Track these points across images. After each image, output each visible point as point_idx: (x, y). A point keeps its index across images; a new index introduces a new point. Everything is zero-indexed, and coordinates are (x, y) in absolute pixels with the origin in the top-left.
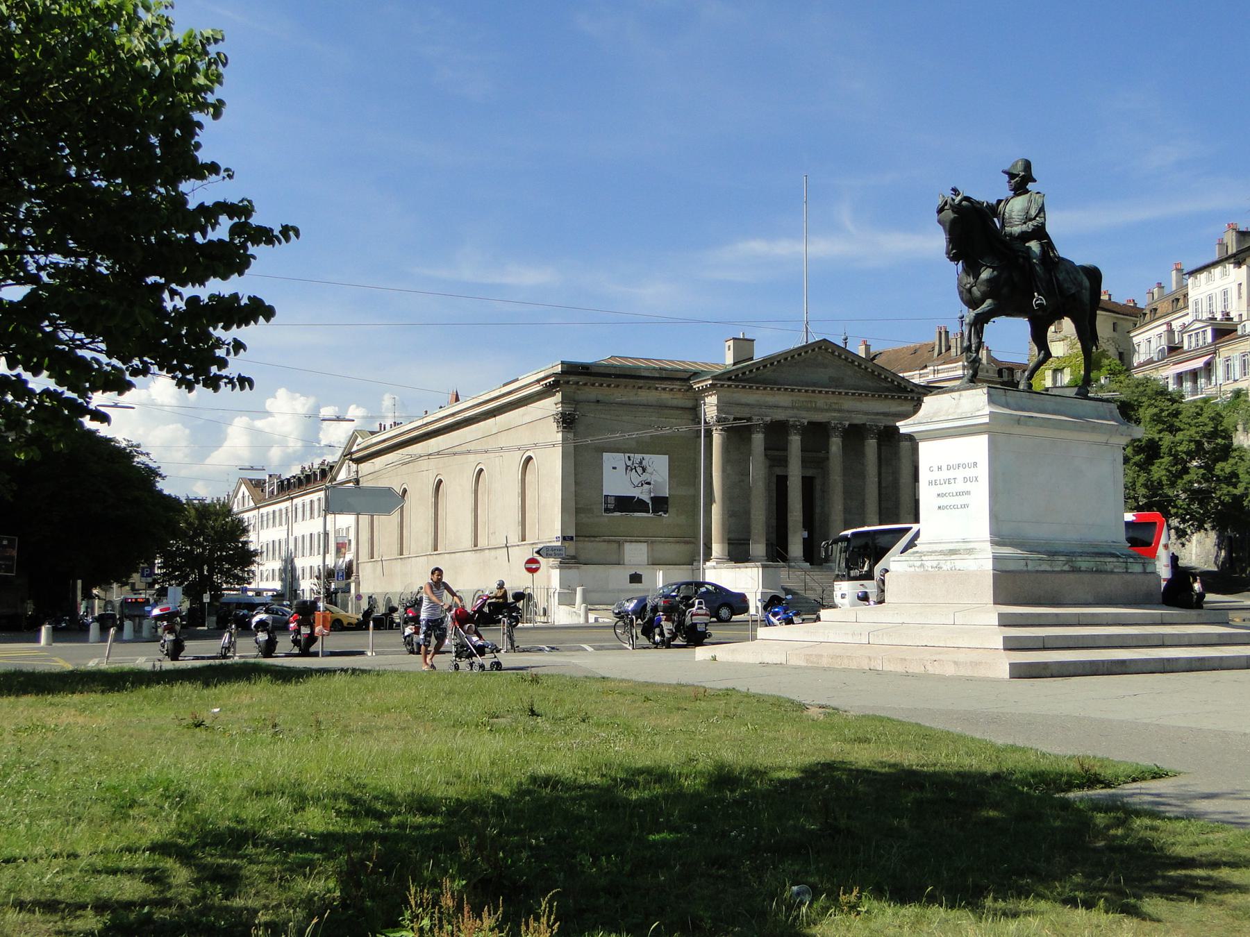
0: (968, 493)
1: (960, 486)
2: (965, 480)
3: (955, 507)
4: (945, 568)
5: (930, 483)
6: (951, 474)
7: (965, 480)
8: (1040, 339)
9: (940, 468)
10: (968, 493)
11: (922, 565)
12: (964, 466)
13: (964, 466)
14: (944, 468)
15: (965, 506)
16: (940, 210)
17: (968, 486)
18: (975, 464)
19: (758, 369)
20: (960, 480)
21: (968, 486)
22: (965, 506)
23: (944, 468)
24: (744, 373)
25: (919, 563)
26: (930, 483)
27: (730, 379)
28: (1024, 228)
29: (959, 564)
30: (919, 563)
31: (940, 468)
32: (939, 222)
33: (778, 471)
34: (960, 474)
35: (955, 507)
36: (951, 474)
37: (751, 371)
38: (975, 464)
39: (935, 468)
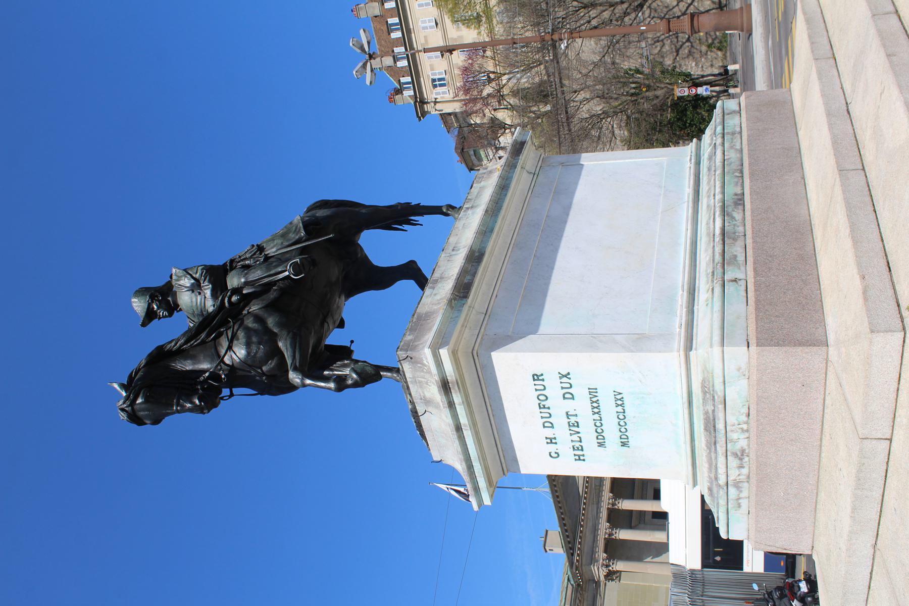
0: (593, 392)
2: (568, 396)
3: (622, 417)
4: (743, 443)
6: (560, 421)
7: (568, 396)
8: (383, 278)
10: (593, 392)
11: (737, 485)
14: (549, 433)
15: (619, 400)
16: (135, 418)
18: (536, 377)
19: (566, 531)
20: (569, 405)
22: (619, 400)
23: (549, 433)
24: (569, 542)
26: (579, 458)
27: (572, 554)
28: (208, 293)
30: (732, 491)
31: (551, 441)
32: (156, 421)
33: (649, 517)
34: (558, 406)
35: (622, 417)
36: (560, 421)
37: (568, 536)
38: (536, 377)
39: (552, 448)
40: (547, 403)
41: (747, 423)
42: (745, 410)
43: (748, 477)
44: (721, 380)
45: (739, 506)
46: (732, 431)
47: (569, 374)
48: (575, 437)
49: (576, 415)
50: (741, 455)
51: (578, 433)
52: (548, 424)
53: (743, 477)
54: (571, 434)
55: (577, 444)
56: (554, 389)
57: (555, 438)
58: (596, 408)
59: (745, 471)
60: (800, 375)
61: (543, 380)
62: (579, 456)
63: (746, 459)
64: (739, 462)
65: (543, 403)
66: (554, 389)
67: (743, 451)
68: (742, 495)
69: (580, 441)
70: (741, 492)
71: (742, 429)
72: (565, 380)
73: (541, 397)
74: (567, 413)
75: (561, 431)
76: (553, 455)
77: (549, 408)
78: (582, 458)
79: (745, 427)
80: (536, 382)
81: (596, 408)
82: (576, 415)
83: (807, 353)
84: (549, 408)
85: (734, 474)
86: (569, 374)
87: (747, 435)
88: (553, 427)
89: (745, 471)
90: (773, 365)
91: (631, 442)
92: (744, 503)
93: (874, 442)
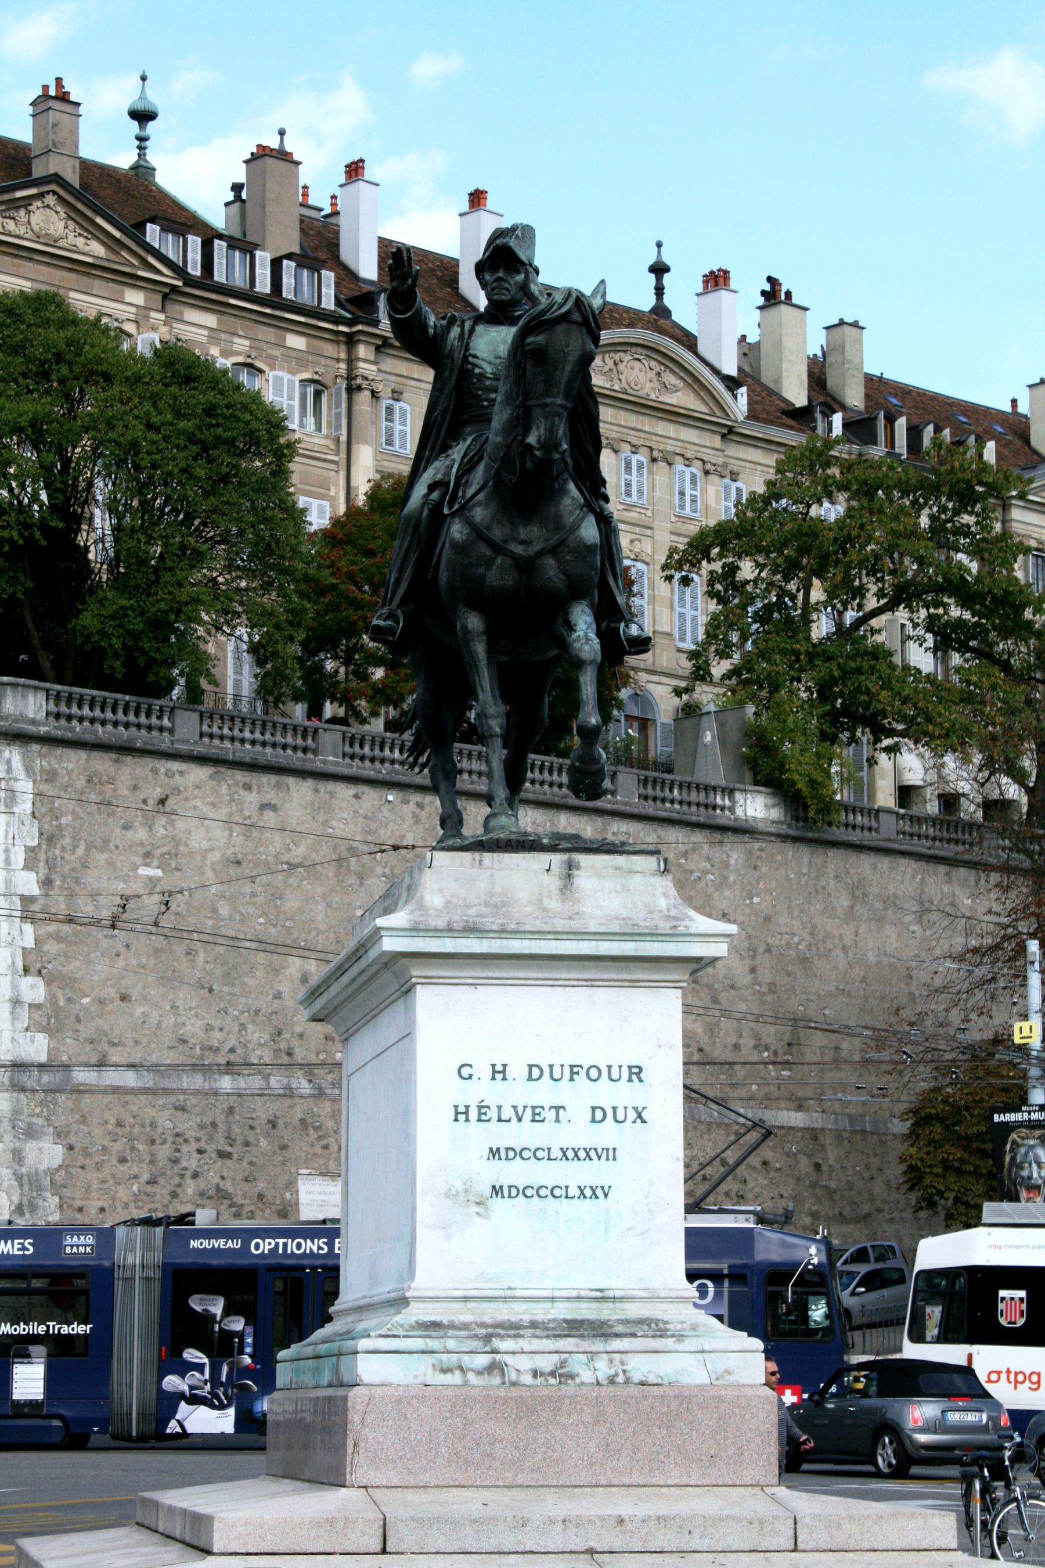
0: (610, 1154)
1: (576, 1132)
2: (597, 1115)
4: (586, 1376)
5: (460, 1113)
6: (544, 1093)
7: (597, 1115)
9: (499, 1072)
10: (610, 1154)
12: (594, 1074)
13: (594, 1074)
14: (517, 1070)
15: (596, 1192)
17: (607, 1135)
18: (636, 1072)
21: (607, 1135)
22: (596, 1192)
23: (517, 1070)
25: (482, 1361)
29: (640, 1367)
31: (499, 1072)
34: (578, 1098)
36: (544, 1093)
40: (581, 1078)
41: (628, 1381)
42: (652, 1380)
43: (514, 1384)
44: (707, 1347)
45: (444, 1371)
46: (611, 1361)
47: (644, 1122)
48: (507, 1113)
49: (557, 1120)
50: (563, 1375)
51: (520, 1120)
52: (534, 1072)
53: (514, 1376)
54: (515, 1107)
55: (493, 1114)
56: (606, 1094)
57: (504, 1079)
58: (571, 1154)
59: (527, 1379)
60: (730, 1452)
61: (630, 1080)
62: (466, 1113)
63: (552, 1381)
64: (548, 1370)
65: (583, 1073)
66: (606, 1094)
67: (572, 1376)
68: (472, 1378)
69: (500, 1120)
70: (479, 1373)
71: (617, 1375)
72: (632, 1115)
73: (594, 1073)
74: (563, 1107)
75: (518, 1092)
76: (465, 1072)
77: (572, 1079)
78: (462, 1117)
79: (620, 1379)
80: (625, 1072)
81: (571, 1154)
82: (557, 1120)
83: (768, 1459)
84: (572, 1079)
85: (524, 1363)
86: (644, 1122)
87: (605, 1382)
88: (530, 1078)
89: (527, 1379)
90: (748, 1417)
91: (498, 1203)
92: (456, 1378)
93: (791, 1533)
